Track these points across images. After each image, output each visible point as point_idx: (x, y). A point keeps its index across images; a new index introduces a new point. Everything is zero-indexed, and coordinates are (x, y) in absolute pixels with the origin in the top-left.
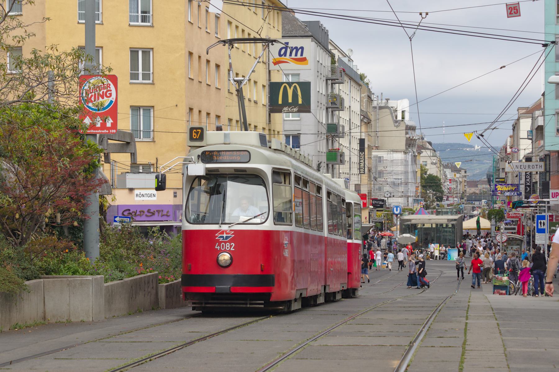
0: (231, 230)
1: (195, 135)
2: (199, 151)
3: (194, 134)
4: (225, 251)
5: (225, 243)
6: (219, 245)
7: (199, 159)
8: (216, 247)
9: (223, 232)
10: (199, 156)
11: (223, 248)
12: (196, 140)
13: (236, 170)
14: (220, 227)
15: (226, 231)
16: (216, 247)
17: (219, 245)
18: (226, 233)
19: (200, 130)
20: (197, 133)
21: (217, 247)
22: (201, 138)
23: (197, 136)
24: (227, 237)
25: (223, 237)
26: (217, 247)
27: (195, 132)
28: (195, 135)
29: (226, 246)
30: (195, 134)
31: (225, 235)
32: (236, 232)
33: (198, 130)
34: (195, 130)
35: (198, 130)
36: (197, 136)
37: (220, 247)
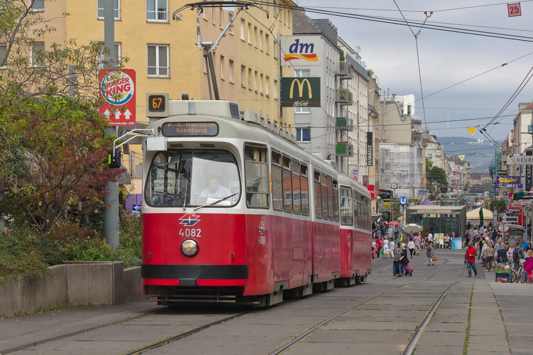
0: (197, 214)
1: (155, 105)
2: (160, 123)
3: (154, 103)
4: (190, 238)
5: (191, 228)
6: (184, 231)
7: (159, 132)
8: (180, 234)
9: (187, 216)
10: (159, 128)
11: (188, 234)
12: (156, 110)
13: (203, 144)
14: (185, 210)
15: (191, 215)
16: (180, 234)
17: (184, 231)
18: (192, 218)
19: (161, 99)
20: (157, 102)
21: (181, 233)
22: (162, 108)
23: (158, 105)
24: (192, 222)
25: (188, 222)
26: (181, 233)
27: (155, 101)
28: (155, 105)
29: (191, 232)
30: (155, 103)
31: (190, 220)
32: (203, 216)
33: (158, 99)
34: (155, 99)
35: (158, 99)
36: (158, 105)
37: (185, 233)
